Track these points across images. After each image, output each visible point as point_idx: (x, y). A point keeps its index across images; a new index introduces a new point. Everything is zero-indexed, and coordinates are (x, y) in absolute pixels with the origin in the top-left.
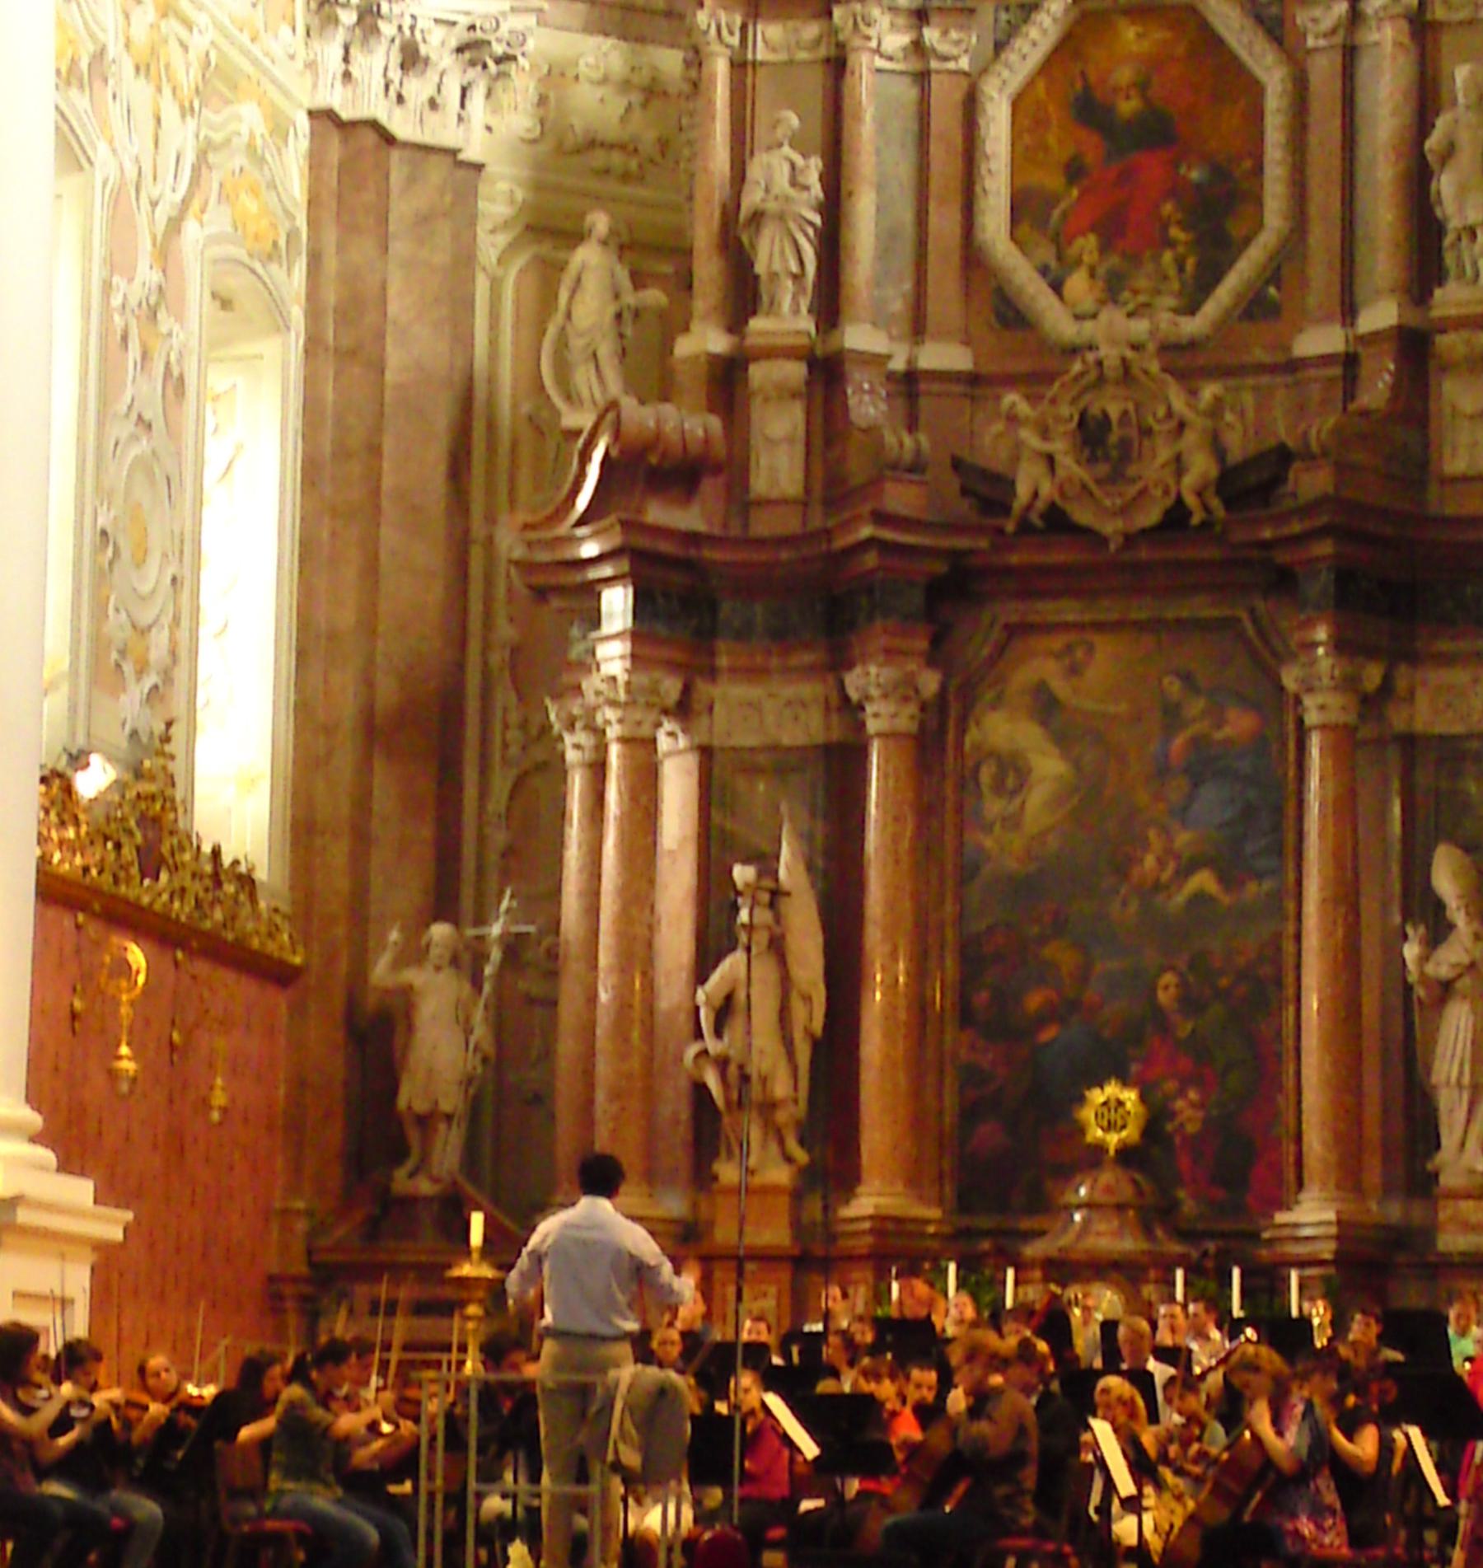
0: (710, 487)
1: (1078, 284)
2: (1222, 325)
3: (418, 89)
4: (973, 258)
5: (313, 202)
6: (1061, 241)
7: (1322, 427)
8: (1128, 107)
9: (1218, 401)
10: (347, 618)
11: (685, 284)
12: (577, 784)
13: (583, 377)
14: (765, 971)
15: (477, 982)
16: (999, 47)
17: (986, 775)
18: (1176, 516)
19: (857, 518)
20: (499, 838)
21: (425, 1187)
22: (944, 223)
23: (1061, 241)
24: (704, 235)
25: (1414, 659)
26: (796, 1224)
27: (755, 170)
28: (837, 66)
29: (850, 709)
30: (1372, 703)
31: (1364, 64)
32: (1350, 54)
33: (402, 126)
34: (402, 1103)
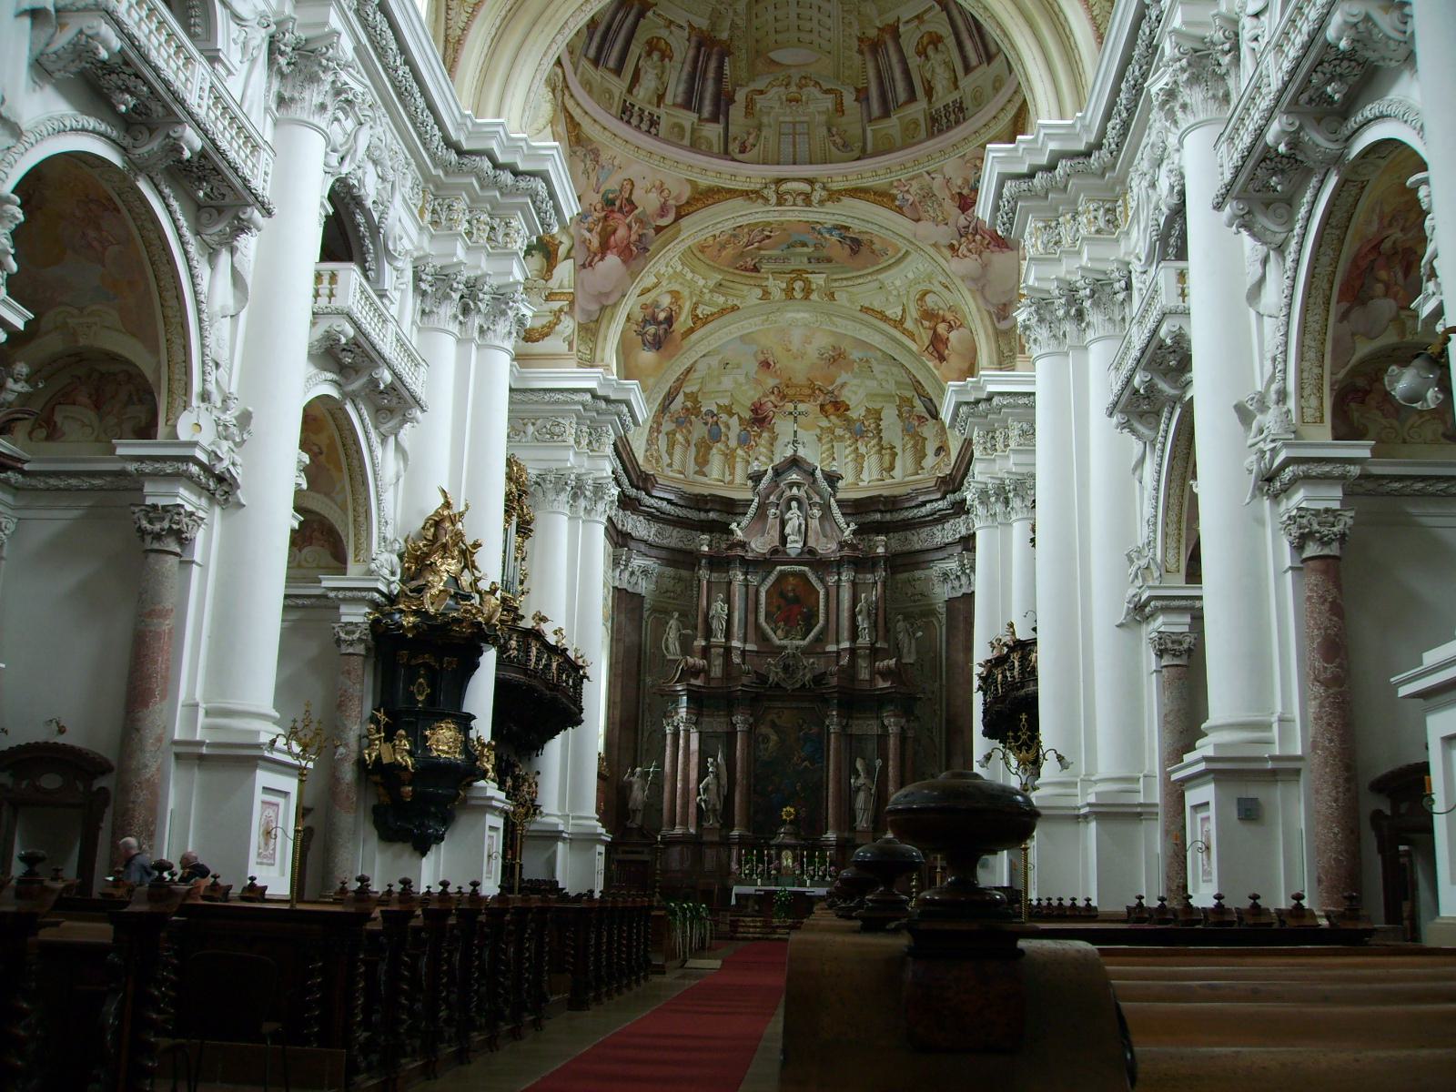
0: (702, 675)
1: (779, 632)
2: (811, 643)
3: (633, 580)
4: (757, 626)
5: (613, 606)
6: (776, 623)
7: (834, 669)
8: (791, 594)
9: (813, 663)
10: (618, 699)
11: (696, 628)
12: (669, 738)
13: (671, 647)
14: (715, 781)
15: (646, 781)
16: (764, 580)
17: (760, 739)
18: (804, 685)
19: (737, 686)
20: (645, 747)
21: (635, 826)
22: (751, 618)
23: (776, 623)
24: (700, 620)
25: (852, 718)
26: (720, 837)
27: (713, 607)
28: (730, 583)
29: (734, 726)
30: (844, 728)
31: (841, 590)
32: (838, 587)
33: (630, 590)
34: (630, 806)
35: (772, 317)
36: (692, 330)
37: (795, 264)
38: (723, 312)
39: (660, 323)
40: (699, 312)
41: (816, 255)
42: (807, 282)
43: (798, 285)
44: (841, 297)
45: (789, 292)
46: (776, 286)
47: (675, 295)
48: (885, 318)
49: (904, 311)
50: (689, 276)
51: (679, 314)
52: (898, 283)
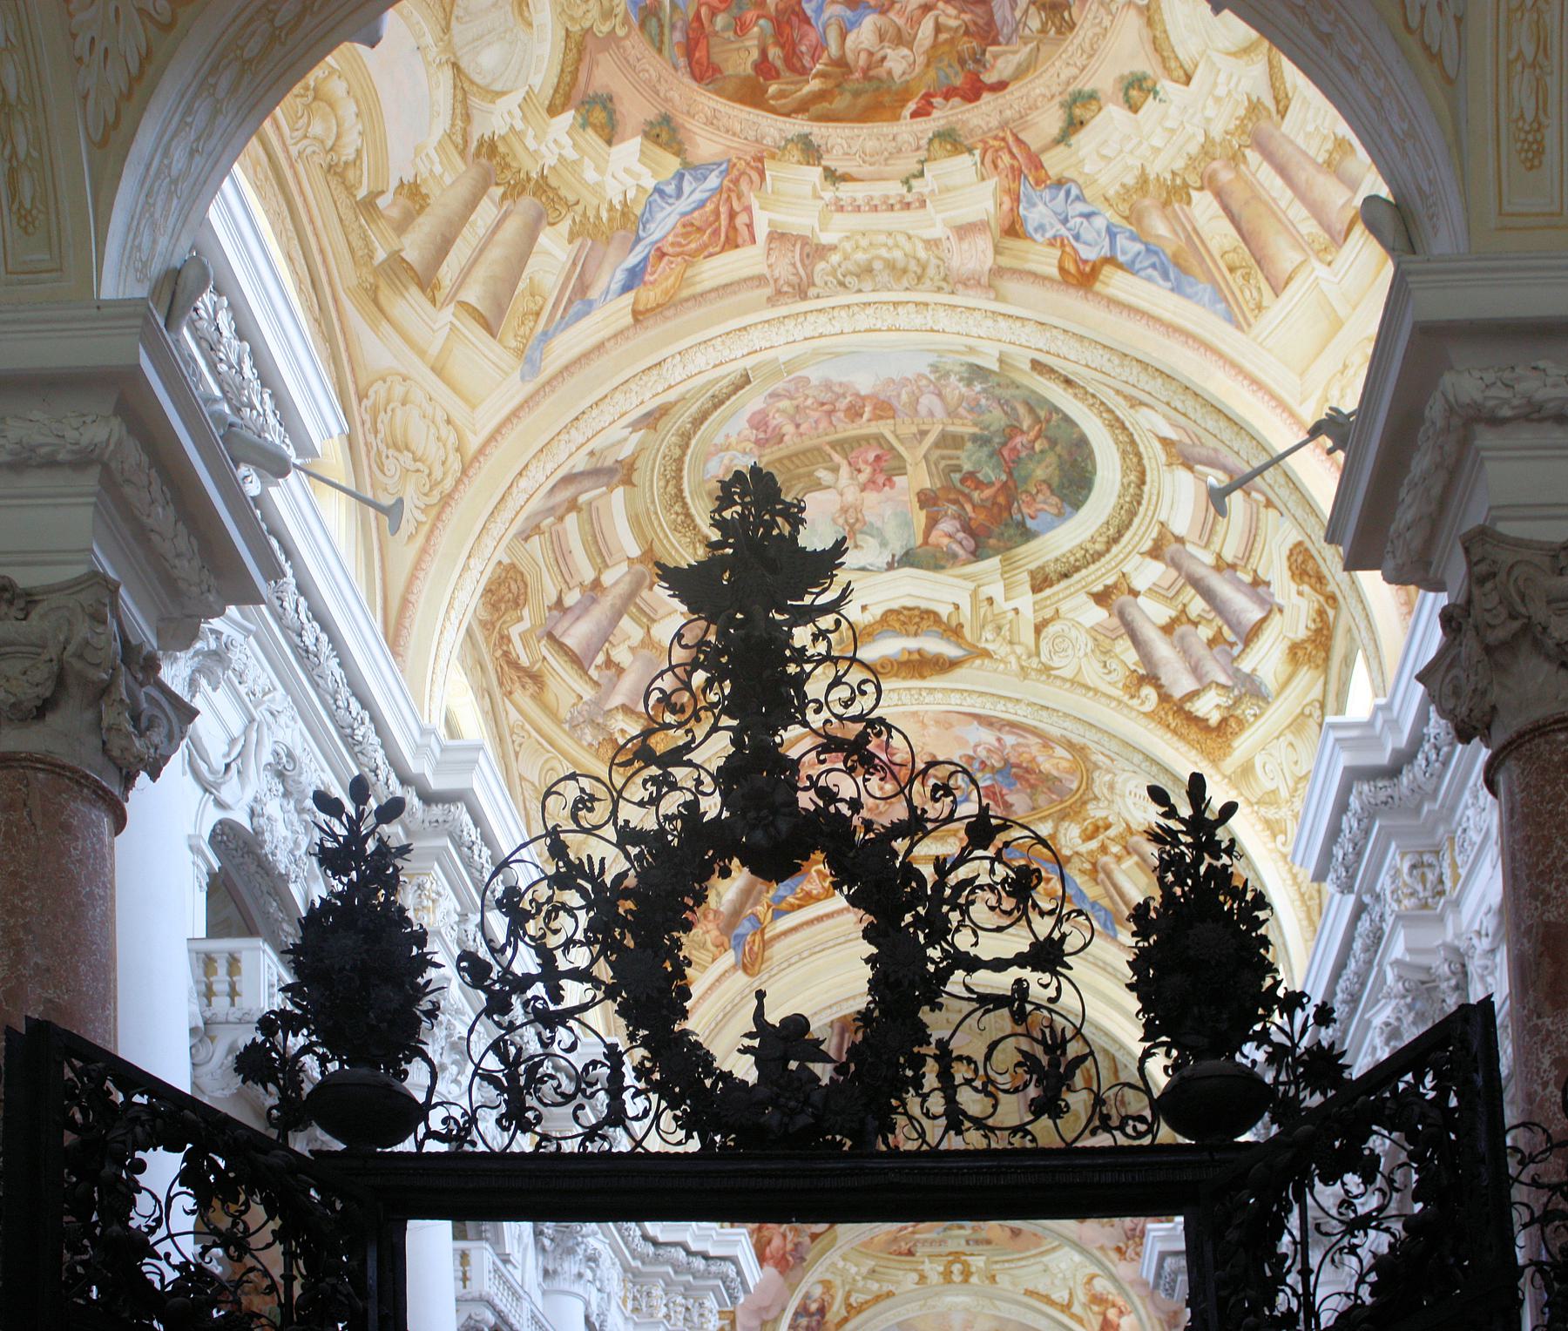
35: (930, 1302)
36: (845, 1320)
37: (952, 1246)
38: (878, 1298)
39: (811, 1315)
40: (852, 1300)
41: (975, 1236)
42: (966, 1264)
43: (957, 1268)
44: (1004, 1281)
45: (947, 1275)
46: (933, 1270)
47: (827, 1285)
48: (1051, 1303)
49: (1071, 1294)
50: (841, 1264)
51: (831, 1305)
52: (1063, 1266)
